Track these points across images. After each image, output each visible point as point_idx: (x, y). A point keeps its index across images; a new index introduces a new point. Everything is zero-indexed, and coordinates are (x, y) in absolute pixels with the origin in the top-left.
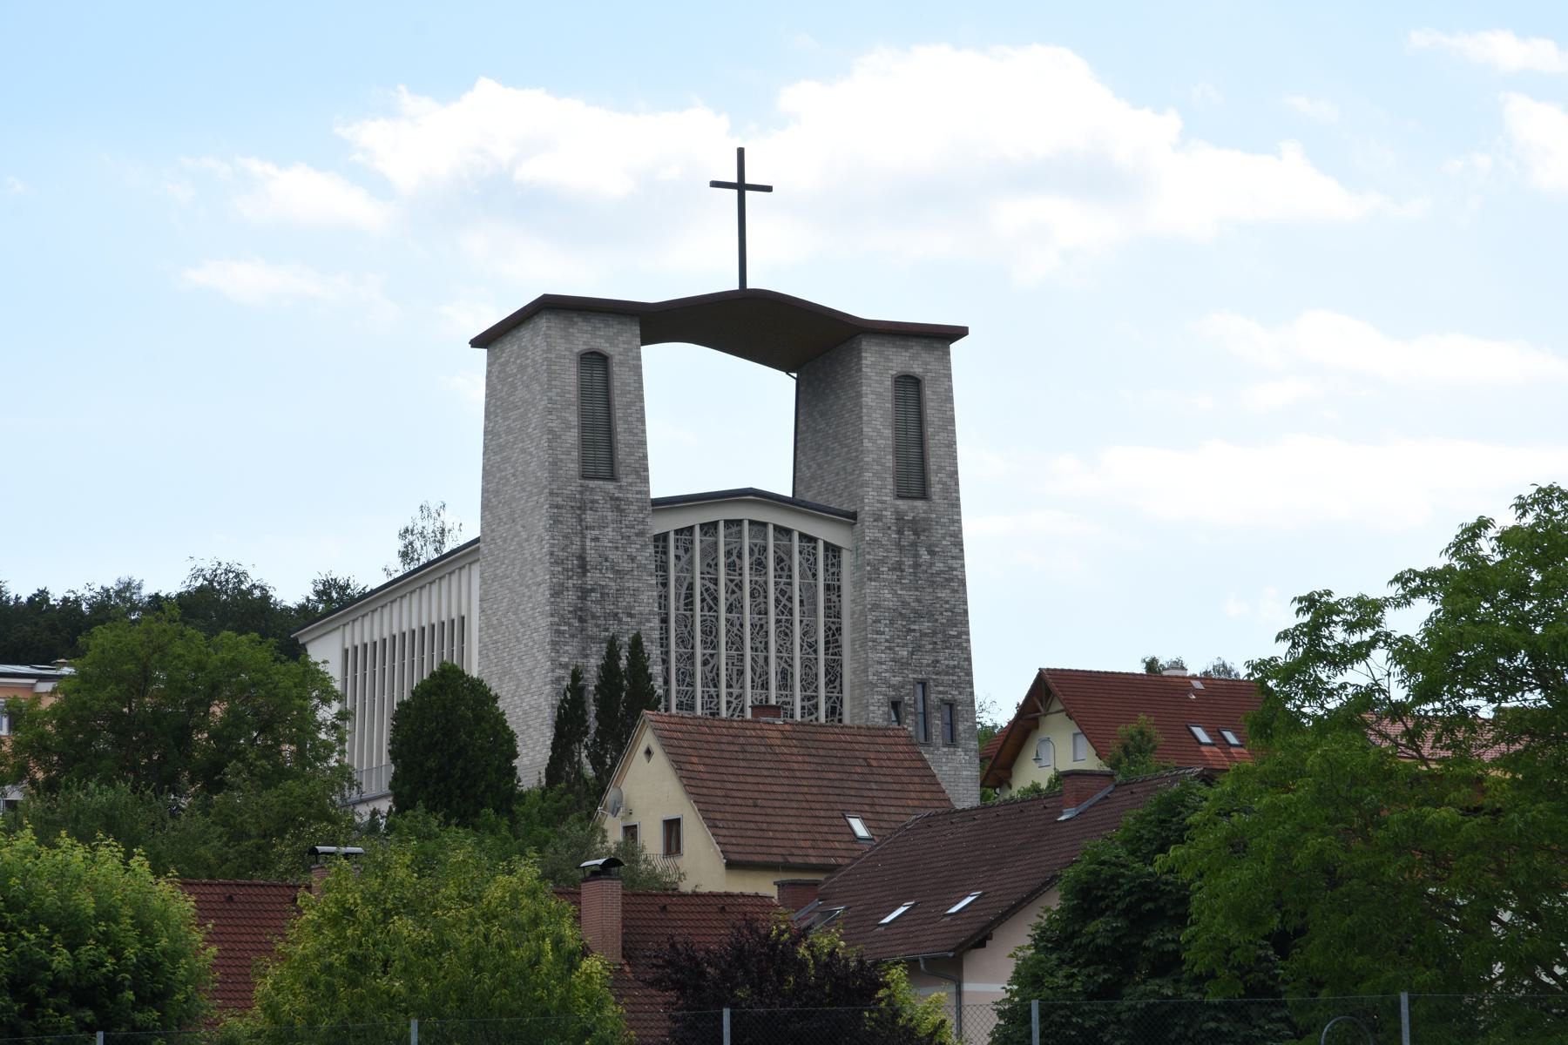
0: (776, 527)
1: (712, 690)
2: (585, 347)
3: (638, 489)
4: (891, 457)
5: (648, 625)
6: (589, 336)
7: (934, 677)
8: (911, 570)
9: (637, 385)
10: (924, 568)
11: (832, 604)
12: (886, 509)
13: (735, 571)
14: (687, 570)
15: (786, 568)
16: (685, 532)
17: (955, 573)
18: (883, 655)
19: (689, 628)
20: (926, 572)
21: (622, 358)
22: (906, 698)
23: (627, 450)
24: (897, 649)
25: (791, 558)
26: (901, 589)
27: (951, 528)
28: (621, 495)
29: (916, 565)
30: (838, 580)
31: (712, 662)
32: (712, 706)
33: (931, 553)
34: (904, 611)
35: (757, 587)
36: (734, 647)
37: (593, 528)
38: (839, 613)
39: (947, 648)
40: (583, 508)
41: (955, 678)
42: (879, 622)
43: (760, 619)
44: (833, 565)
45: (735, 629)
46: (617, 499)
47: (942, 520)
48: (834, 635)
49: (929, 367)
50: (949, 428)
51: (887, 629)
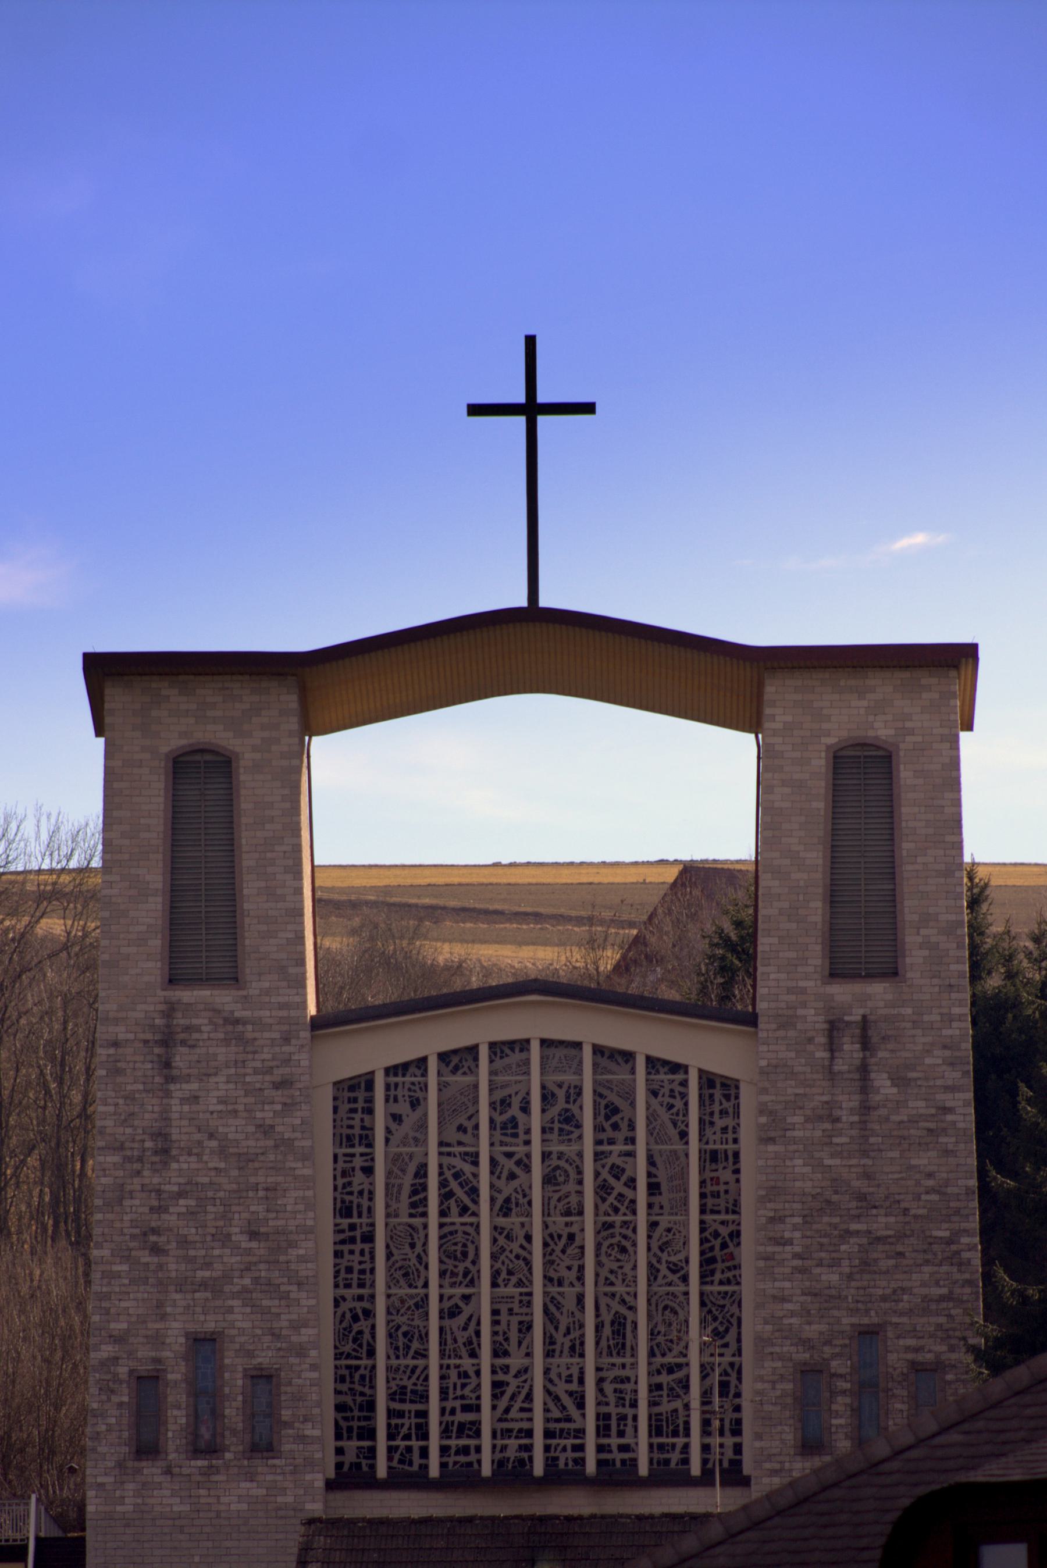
0: (598, 1050)
1: (467, 1363)
2: (183, 742)
3: (281, 999)
4: (819, 904)
5: (293, 1252)
6: (192, 721)
7: (895, 1320)
8: (856, 1118)
9: (287, 805)
10: (883, 1112)
11: (722, 1188)
12: (804, 1005)
13: (515, 1135)
14: (416, 1139)
15: (624, 1125)
16: (412, 1069)
17: (949, 1118)
18: (787, 1284)
19: (419, 1249)
20: (887, 1119)
21: (258, 756)
22: (834, 1363)
23: (264, 928)
24: (817, 1271)
25: (633, 1104)
26: (832, 1156)
27: (947, 1032)
28: (247, 1014)
29: (866, 1108)
30: (736, 1141)
31: (467, 1311)
32: (467, 1391)
33: (899, 1081)
34: (835, 1198)
35: (562, 1163)
36: (514, 1280)
37: (187, 1079)
38: (736, 1203)
39: (927, 1262)
40: (167, 1042)
41: (942, 1320)
42: (781, 1220)
43: (567, 1224)
44: (723, 1113)
45: (515, 1246)
46: (237, 1021)
47: (926, 1018)
48: (724, 1246)
49: (908, 724)
50: (949, 838)
51: (797, 1234)
